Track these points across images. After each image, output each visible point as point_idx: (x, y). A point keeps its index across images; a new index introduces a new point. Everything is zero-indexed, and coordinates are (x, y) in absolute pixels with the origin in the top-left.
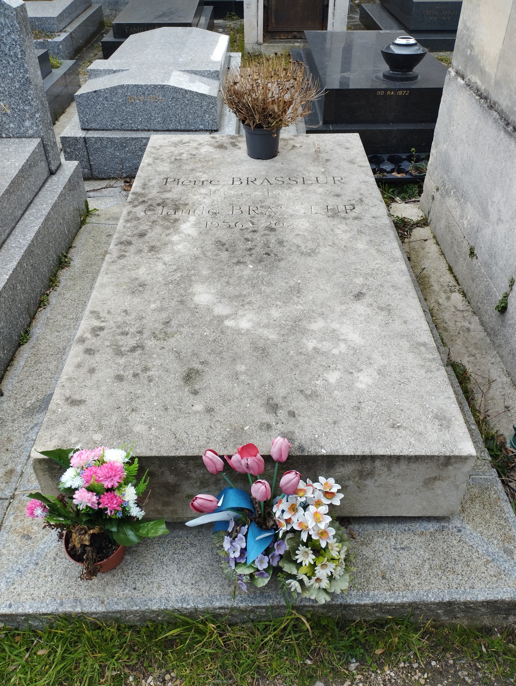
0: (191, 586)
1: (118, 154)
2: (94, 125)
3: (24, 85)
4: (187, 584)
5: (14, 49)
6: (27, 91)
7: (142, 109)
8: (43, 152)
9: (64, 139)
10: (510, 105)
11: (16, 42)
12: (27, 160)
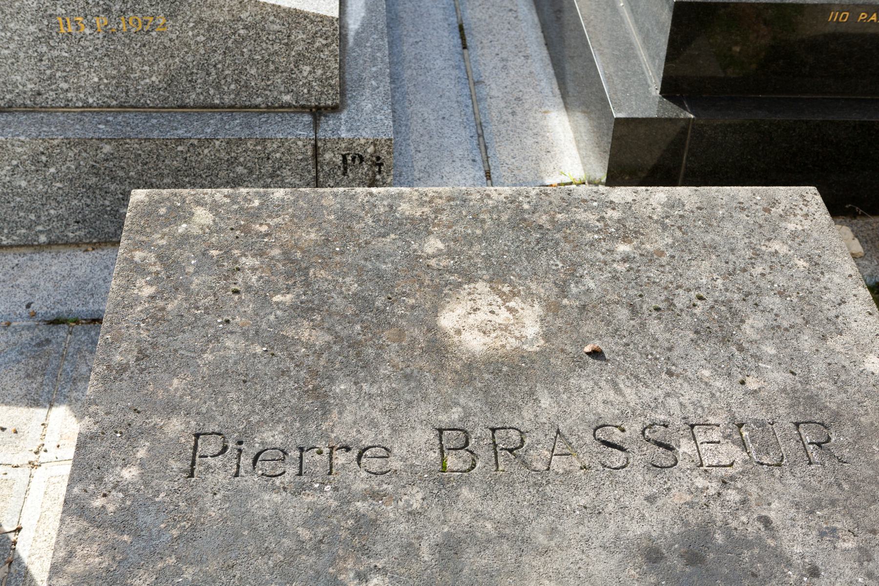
1: (24, 184)
7: (102, 51)
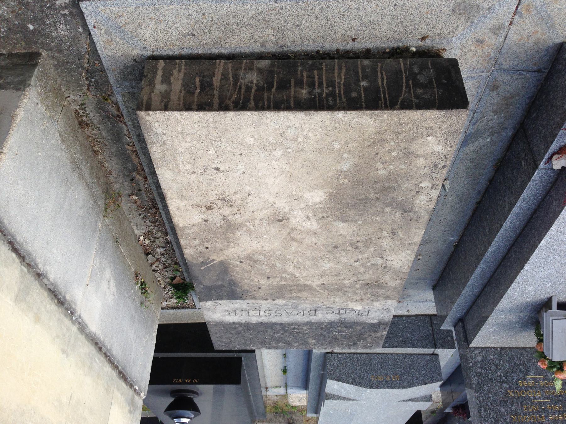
0: (352, 7)
2: (428, 358)
3: (480, 388)
4: (355, 8)
5: (487, 415)
6: (478, 383)
8: (468, 336)
9: (452, 347)
10: (104, 368)
11: (485, 419)
12: (480, 330)
